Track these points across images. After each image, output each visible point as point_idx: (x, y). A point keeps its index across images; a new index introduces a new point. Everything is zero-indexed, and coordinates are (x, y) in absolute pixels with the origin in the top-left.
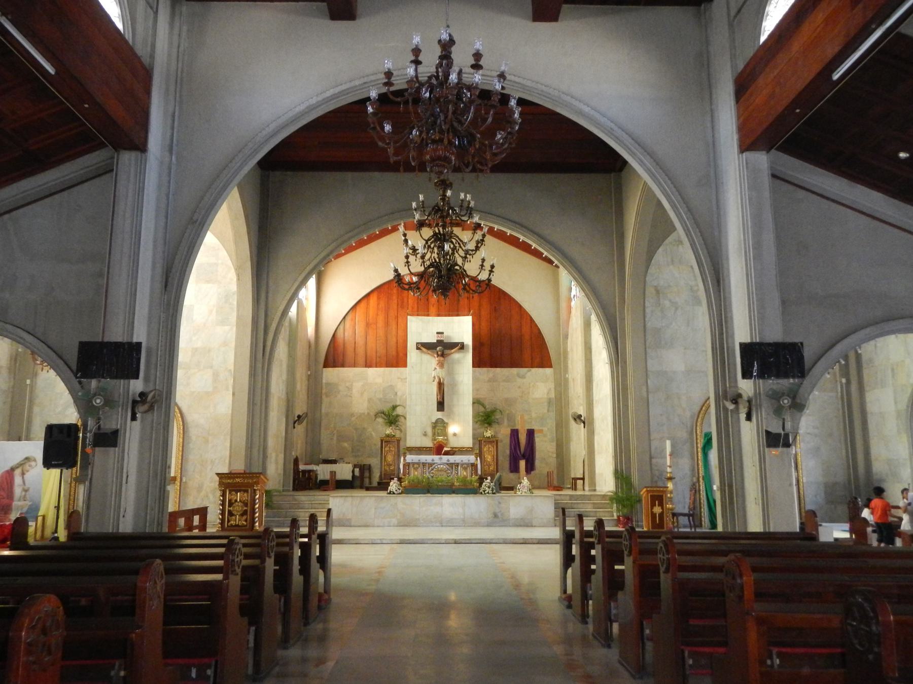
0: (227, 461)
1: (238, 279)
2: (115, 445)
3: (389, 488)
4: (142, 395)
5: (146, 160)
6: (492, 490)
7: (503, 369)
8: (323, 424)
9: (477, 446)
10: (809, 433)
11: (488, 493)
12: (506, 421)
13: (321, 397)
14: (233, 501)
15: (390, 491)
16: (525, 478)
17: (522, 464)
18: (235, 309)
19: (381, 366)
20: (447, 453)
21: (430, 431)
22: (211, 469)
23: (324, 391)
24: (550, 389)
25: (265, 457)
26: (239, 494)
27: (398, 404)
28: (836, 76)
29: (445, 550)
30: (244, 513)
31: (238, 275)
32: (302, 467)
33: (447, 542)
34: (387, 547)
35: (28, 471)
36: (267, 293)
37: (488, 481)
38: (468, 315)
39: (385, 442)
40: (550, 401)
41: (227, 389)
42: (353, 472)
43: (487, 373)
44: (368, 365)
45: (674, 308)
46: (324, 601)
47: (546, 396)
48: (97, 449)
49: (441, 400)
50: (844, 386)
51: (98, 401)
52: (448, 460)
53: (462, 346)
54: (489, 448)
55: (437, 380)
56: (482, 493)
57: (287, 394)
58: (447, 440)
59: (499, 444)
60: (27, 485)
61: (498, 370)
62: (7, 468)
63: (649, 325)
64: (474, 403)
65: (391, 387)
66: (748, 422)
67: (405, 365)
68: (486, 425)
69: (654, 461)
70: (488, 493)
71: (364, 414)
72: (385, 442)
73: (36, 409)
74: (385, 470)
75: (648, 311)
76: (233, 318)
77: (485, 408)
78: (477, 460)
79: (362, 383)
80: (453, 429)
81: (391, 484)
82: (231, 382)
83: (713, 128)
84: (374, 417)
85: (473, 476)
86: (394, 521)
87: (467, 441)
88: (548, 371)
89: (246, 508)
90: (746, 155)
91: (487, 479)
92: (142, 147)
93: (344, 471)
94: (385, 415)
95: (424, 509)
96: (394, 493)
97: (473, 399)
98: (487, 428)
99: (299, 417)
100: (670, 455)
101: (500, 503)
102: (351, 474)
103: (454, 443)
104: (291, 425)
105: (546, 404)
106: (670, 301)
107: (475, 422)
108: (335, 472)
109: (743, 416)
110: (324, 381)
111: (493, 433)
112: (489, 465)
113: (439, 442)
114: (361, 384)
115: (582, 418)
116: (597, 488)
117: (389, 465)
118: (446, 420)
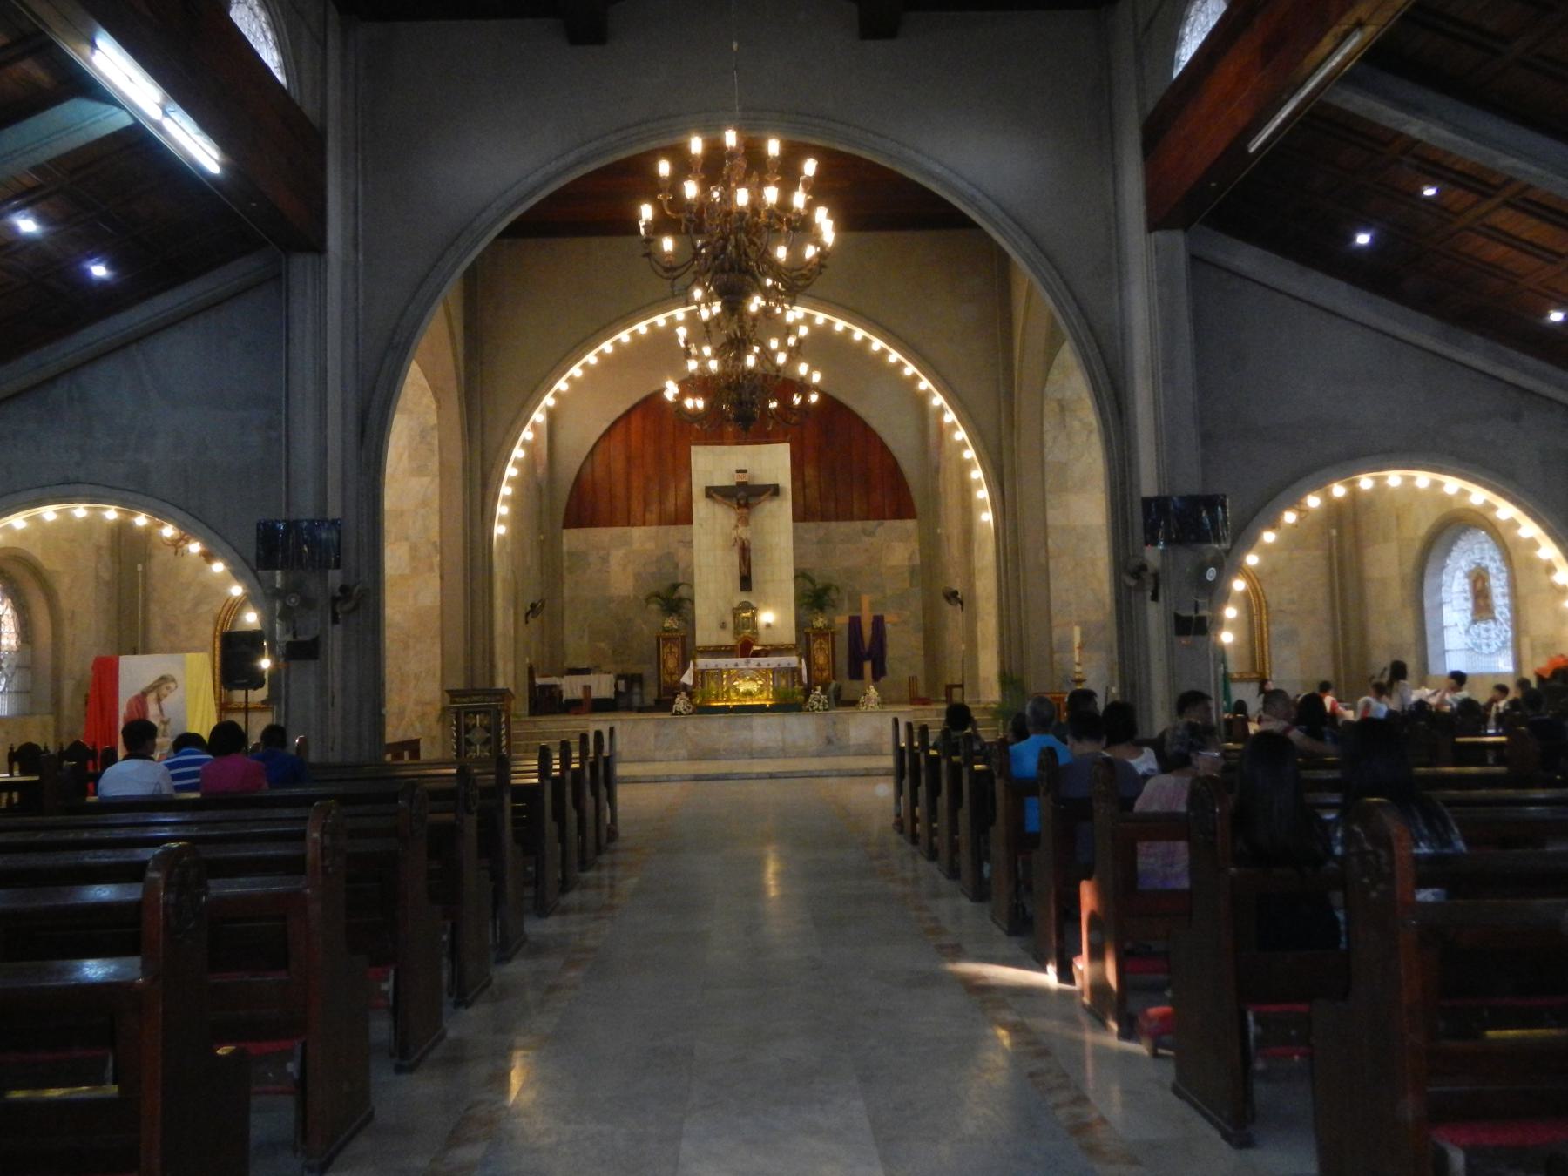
0: (438, 674)
1: (439, 408)
2: (316, 658)
3: (675, 706)
4: (344, 589)
5: (326, 263)
6: (824, 706)
8: (567, 614)
9: (804, 641)
10: (1281, 611)
11: (818, 709)
12: (846, 602)
13: (562, 575)
14: (470, 726)
15: (676, 711)
16: (872, 687)
17: (868, 666)
18: (437, 453)
20: (756, 654)
21: (729, 620)
22: (415, 686)
23: (566, 564)
24: (913, 551)
25: (492, 666)
26: (478, 717)
27: (680, 580)
28: (1252, 150)
29: (756, 786)
30: (486, 742)
31: (438, 401)
32: (539, 681)
33: (759, 777)
34: (676, 787)
35: (165, 696)
36: (483, 425)
37: (817, 692)
38: (784, 442)
39: (664, 639)
40: (913, 570)
41: (431, 569)
42: (616, 686)
43: (815, 529)
44: (629, 523)
45: (1086, 432)
46: (613, 835)
47: (906, 563)
48: (294, 664)
49: (746, 572)
50: (1334, 540)
51: (293, 600)
52: (759, 665)
53: (775, 491)
54: (821, 644)
55: (739, 542)
56: (808, 710)
57: (513, 572)
58: (756, 634)
59: (837, 637)
60: (167, 716)
61: (833, 524)
62: (137, 692)
63: (1049, 458)
64: (796, 577)
65: (670, 556)
66: (1154, 602)
67: (688, 520)
68: (816, 610)
69: (1057, 657)
70: (818, 709)
71: (629, 597)
72: (664, 639)
73: (154, 608)
74: (665, 682)
75: (1048, 438)
76: (434, 465)
77: (812, 581)
78: (800, 662)
80: (766, 617)
81: (678, 699)
82: (437, 559)
83: (1115, 192)
84: (644, 602)
85: (797, 686)
86: (683, 753)
87: (788, 636)
88: (910, 524)
89: (489, 735)
90: (1158, 235)
91: (815, 690)
92: (317, 247)
93: (603, 686)
94: (662, 599)
95: (725, 735)
96: (681, 714)
97: (796, 570)
99: (533, 606)
100: (1080, 648)
101: (835, 723)
102: (614, 689)
103: (765, 639)
104: (522, 619)
105: (907, 575)
106: (1080, 420)
107: (798, 606)
108: (590, 687)
109: (1149, 594)
110: (565, 548)
111: (826, 622)
112: (822, 670)
113: (745, 637)
114: (622, 552)
115: (959, 596)
116: (982, 699)
117: (671, 674)
118: (754, 603)
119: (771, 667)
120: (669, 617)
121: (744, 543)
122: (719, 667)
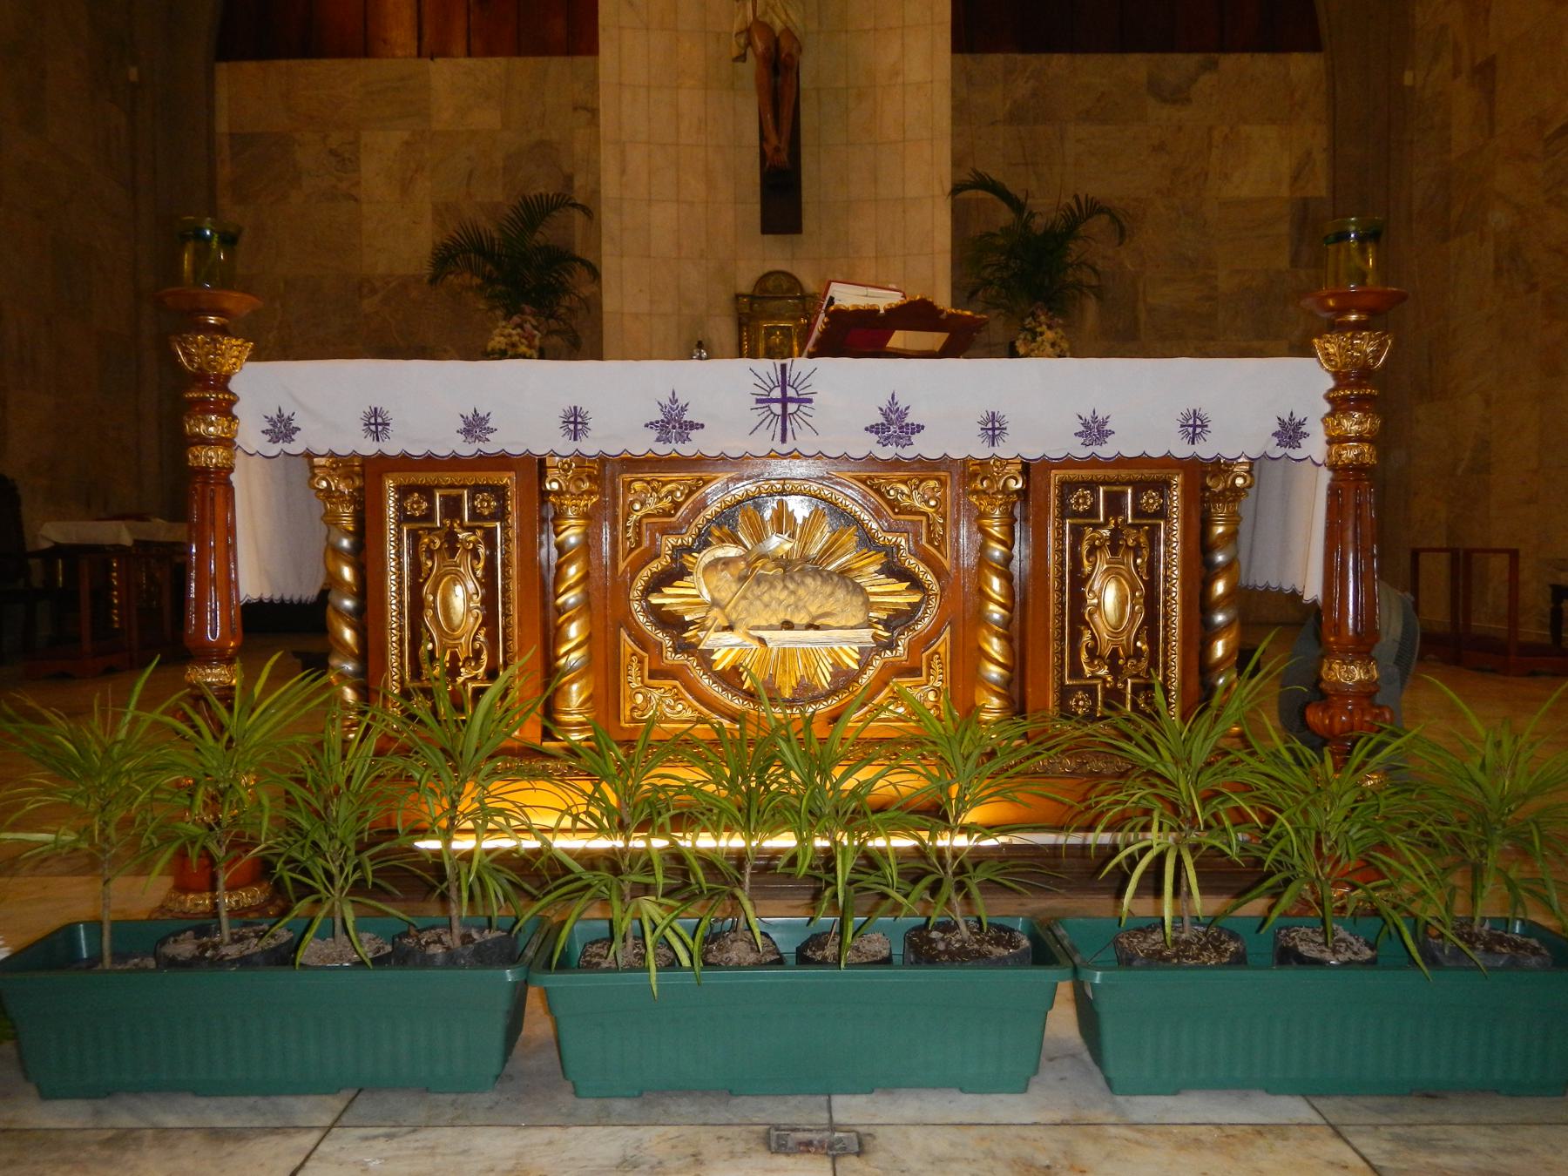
7: (1079, 59)
19: (490, 51)
23: (225, 172)
24: (1309, 154)
47: (1285, 192)
49: (784, 157)
52: (893, 424)
61: (1059, 63)
64: (957, 189)
77: (1016, 204)
79: (406, 135)
88: (1303, 67)
98: (1033, 315)
105: (1284, 228)
110: (222, 126)
118: (810, 284)
119: (1020, 444)
120: (508, 317)
121: (777, 41)
122: (505, 439)
